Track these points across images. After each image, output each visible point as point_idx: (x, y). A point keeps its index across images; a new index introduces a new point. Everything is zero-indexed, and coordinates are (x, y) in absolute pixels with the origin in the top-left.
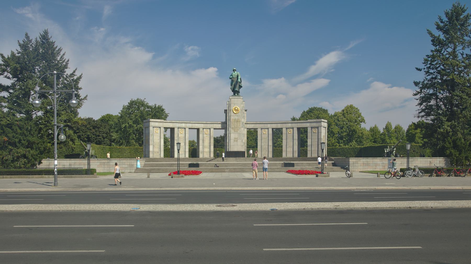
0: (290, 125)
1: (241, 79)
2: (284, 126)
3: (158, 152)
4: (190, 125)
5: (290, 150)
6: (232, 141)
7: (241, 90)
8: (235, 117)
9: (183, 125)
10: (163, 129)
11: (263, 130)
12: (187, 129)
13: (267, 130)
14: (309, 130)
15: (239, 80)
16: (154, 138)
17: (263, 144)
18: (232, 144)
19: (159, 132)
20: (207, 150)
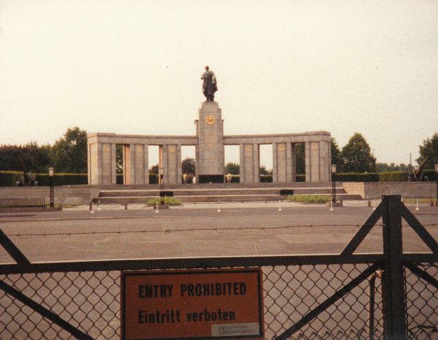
0: (281, 139)
1: (215, 80)
6: (206, 161)
7: (216, 94)
13: (251, 146)
14: (307, 146)
15: (213, 82)
20: (173, 173)
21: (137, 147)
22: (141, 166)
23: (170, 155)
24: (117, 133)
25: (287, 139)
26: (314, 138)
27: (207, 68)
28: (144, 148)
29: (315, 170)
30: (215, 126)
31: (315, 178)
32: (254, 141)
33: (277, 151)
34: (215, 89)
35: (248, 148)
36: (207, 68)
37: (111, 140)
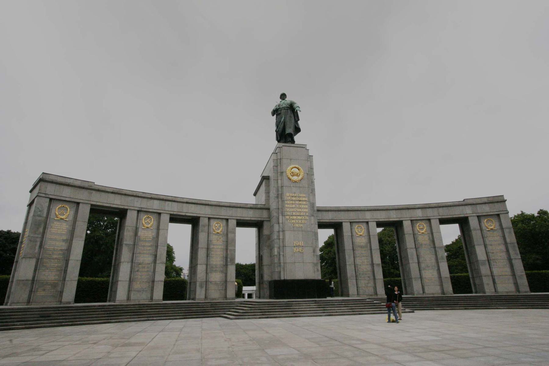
0: (419, 214)
2: (405, 217)
3: (54, 286)
4: (175, 209)
5: (430, 274)
6: (288, 251)
8: (294, 189)
9: (155, 205)
10: (85, 212)
11: (354, 224)
12: (165, 218)
16: (48, 235)
17: (358, 261)
18: (288, 260)
19: (71, 218)
20: (216, 277)
21: (144, 217)
22: (148, 259)
23: (213, 238)
24: (100, 181)
25: (430, 213)
26: (486, 209)
27: (283, 96)
28: (159, 218)
29: (501, 268)
30: (305, 183)
31: (506, 287)
32: (368, 216)
33: (414, 235)
34: (297, 130)
35: (360, 230)
36: (283, 96)
37: (81, 196)
